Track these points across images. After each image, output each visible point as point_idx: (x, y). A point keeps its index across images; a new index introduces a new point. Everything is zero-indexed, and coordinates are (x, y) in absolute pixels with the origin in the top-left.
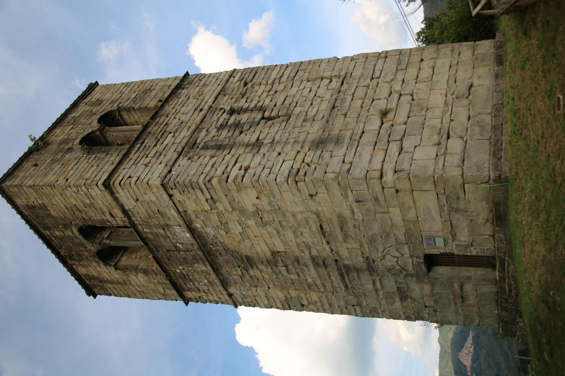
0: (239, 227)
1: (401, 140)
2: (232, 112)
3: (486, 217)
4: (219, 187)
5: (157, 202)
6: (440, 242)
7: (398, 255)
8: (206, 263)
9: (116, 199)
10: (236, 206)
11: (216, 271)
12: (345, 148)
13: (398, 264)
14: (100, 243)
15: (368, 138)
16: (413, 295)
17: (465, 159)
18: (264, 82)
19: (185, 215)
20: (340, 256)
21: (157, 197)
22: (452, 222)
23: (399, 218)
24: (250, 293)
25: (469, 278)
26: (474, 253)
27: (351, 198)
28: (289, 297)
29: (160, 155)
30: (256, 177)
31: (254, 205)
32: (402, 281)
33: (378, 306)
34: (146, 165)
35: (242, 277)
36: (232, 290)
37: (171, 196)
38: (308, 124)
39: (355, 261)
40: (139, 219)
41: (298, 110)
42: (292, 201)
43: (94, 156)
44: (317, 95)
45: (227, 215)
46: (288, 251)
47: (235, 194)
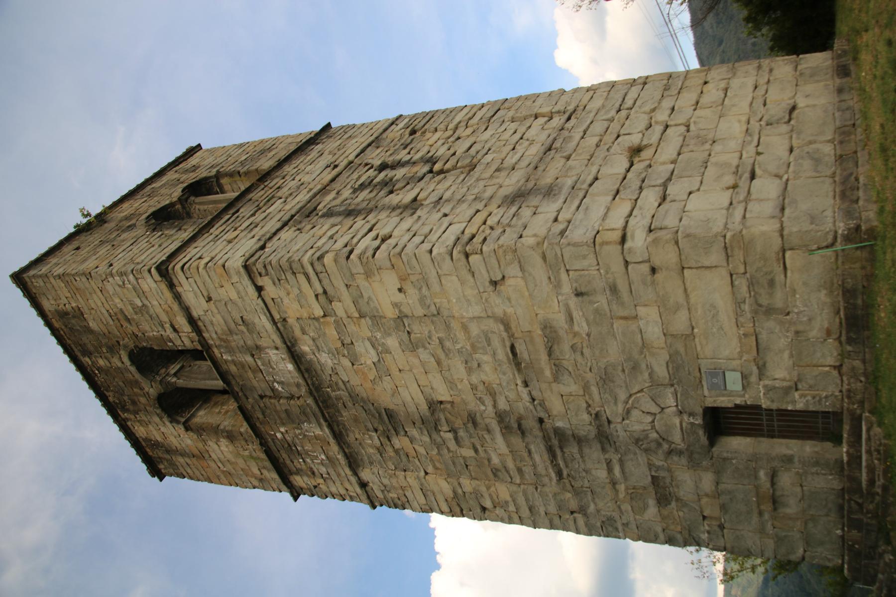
0: (373, 352)
1: (665, 185)
2: (383, 167)
3: (826, 325)
4: (335, 269)
5: (239, 301)
6: (734, 381)
7: (654, 409)
8: (322, 421)
9: (178, 297)
10: (365, 309)
11: (339, 437)
12: (561, 200)
13: (653, 427)
14: (161, 381)
15: (606, 185)
16: (681, 494)
17: (786, 205)
18: (442, 126)
19: (284, 326)
20: (546, 411)
21: (238, 293)
22: (760, 337)
24: (394, 481)
25: (788, 460)
26: (800, 406)
27: (567, 289)
28: (460, 491)
29: (256, 227)
30: (398, 249)
31: (395, 305)
32: (661, 463)
33: (616, 515)
34: (230, 242)
35: (381, 451)
36: (366, 475)
37: (259, 289)
38: (503, 174)
39: (574, 421)
40: (214, 336)
41: (489, 158)
42: (460, 296)
43: (160, 233)
44: (525, 137)
45: (352, 328)
46: (457, 400)
47: (361, 281)
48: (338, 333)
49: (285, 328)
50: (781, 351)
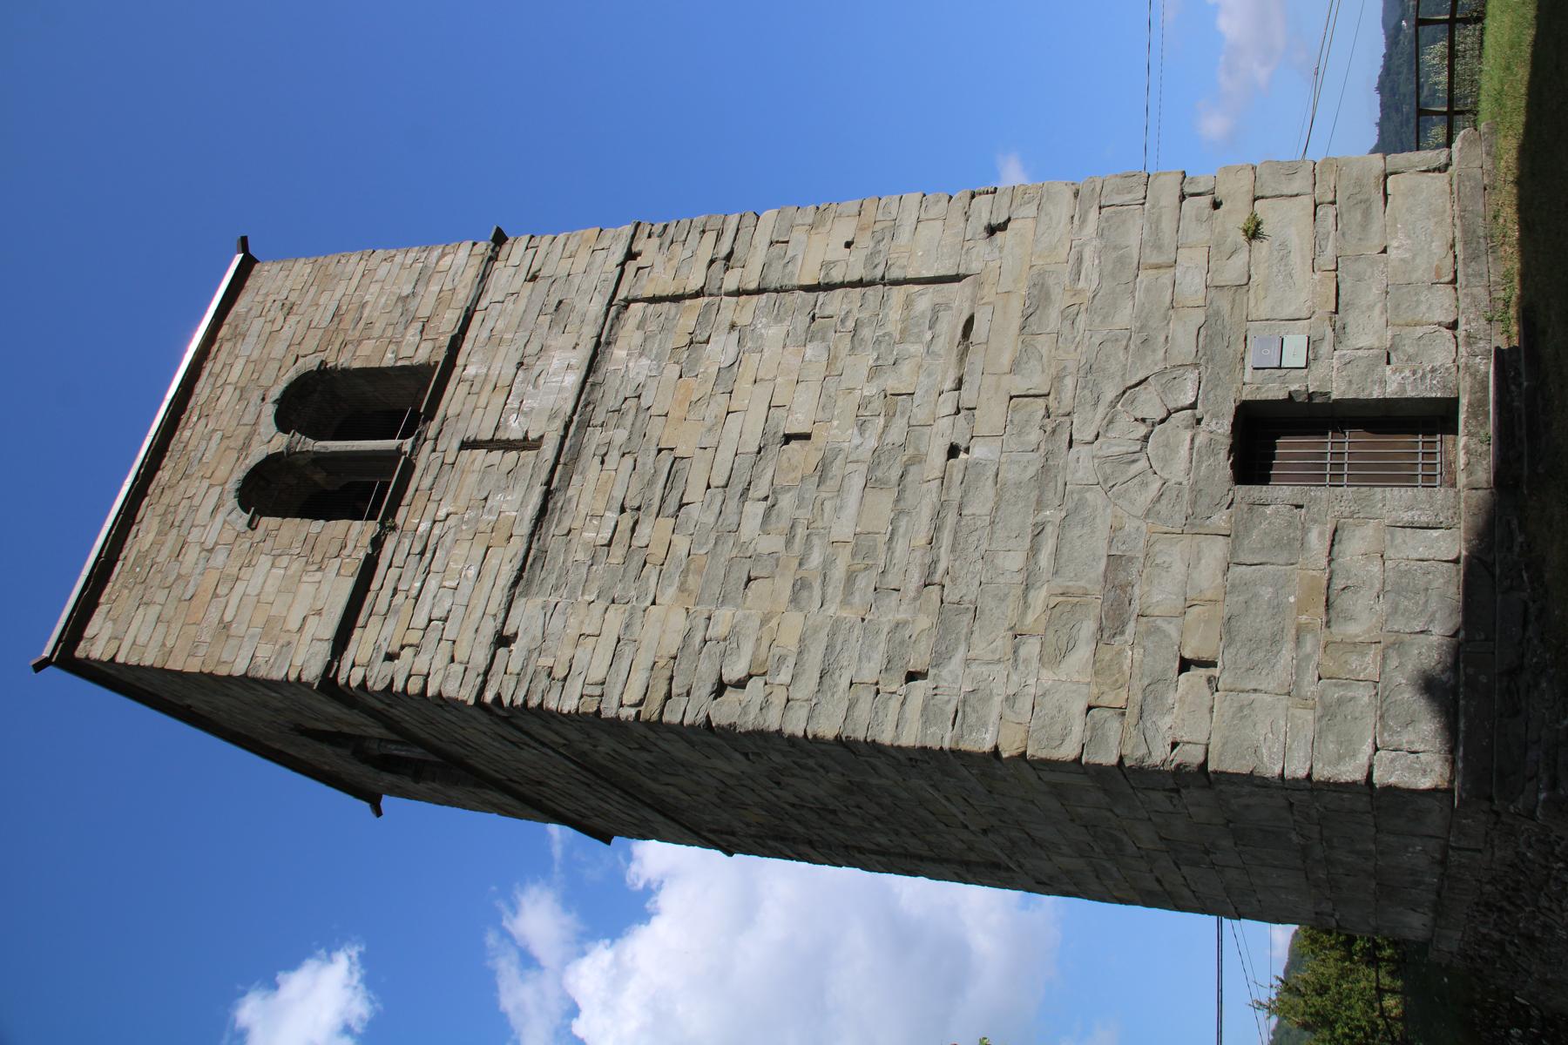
6: (1295, 354)
23: (1197, 280)
49: (617, 317)
50: (1371, 307)
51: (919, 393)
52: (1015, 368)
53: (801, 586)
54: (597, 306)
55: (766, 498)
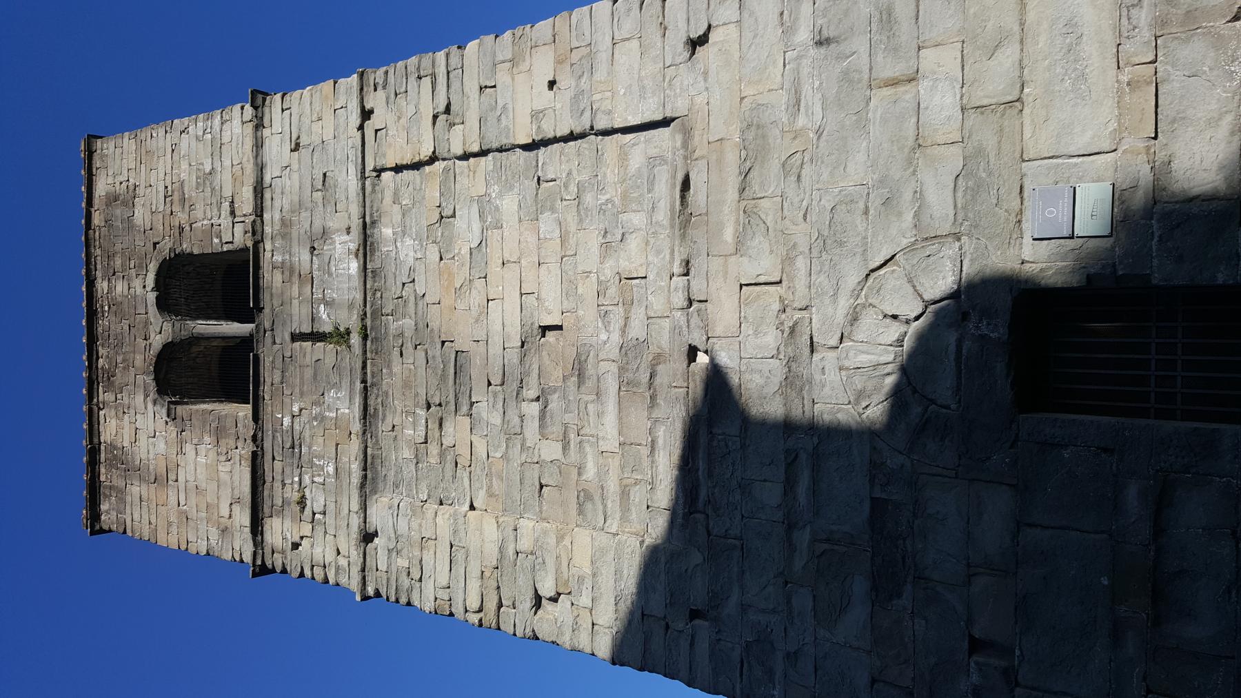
9: (258, 145)
27: (804, 35)
48: (441, 194)
49: (374, 191)
51: (651, 277)
52: (739, 247)
53: (584, 498)
54: (353, 183)
55: (538, 399)
